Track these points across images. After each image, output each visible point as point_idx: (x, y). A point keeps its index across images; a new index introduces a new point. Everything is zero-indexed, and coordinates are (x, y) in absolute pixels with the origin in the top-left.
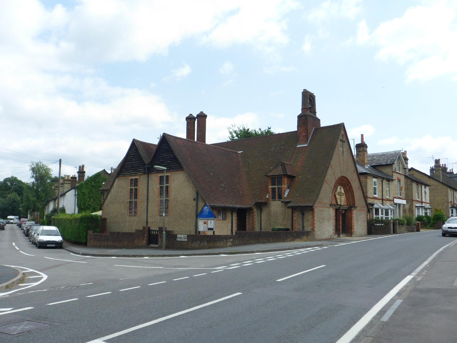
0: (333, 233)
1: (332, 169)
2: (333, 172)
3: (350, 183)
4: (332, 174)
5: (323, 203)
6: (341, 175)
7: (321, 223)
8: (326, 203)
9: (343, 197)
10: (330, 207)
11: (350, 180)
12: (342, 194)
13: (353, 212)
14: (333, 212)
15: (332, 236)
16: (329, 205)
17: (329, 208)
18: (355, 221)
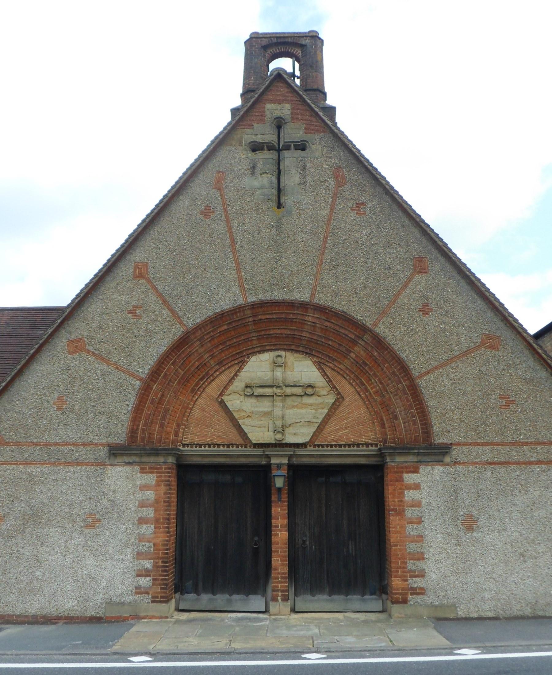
0: (137, 593)
1: (149, 280)
2: (160, 295)
3: (364, 329)
4: (136, 307)
5: (37, 444)
6: (251, 299)
7: (11, 537)
8: (75, 444)
9: (311, 405)
10: (107, 461)
11: (359, 315)
12: (299, 391)
13: (401, 480)
14: (138, 483)
15: (123, 604)
16: (103, 452)
17: (98, 464)
18: (426, 524)
